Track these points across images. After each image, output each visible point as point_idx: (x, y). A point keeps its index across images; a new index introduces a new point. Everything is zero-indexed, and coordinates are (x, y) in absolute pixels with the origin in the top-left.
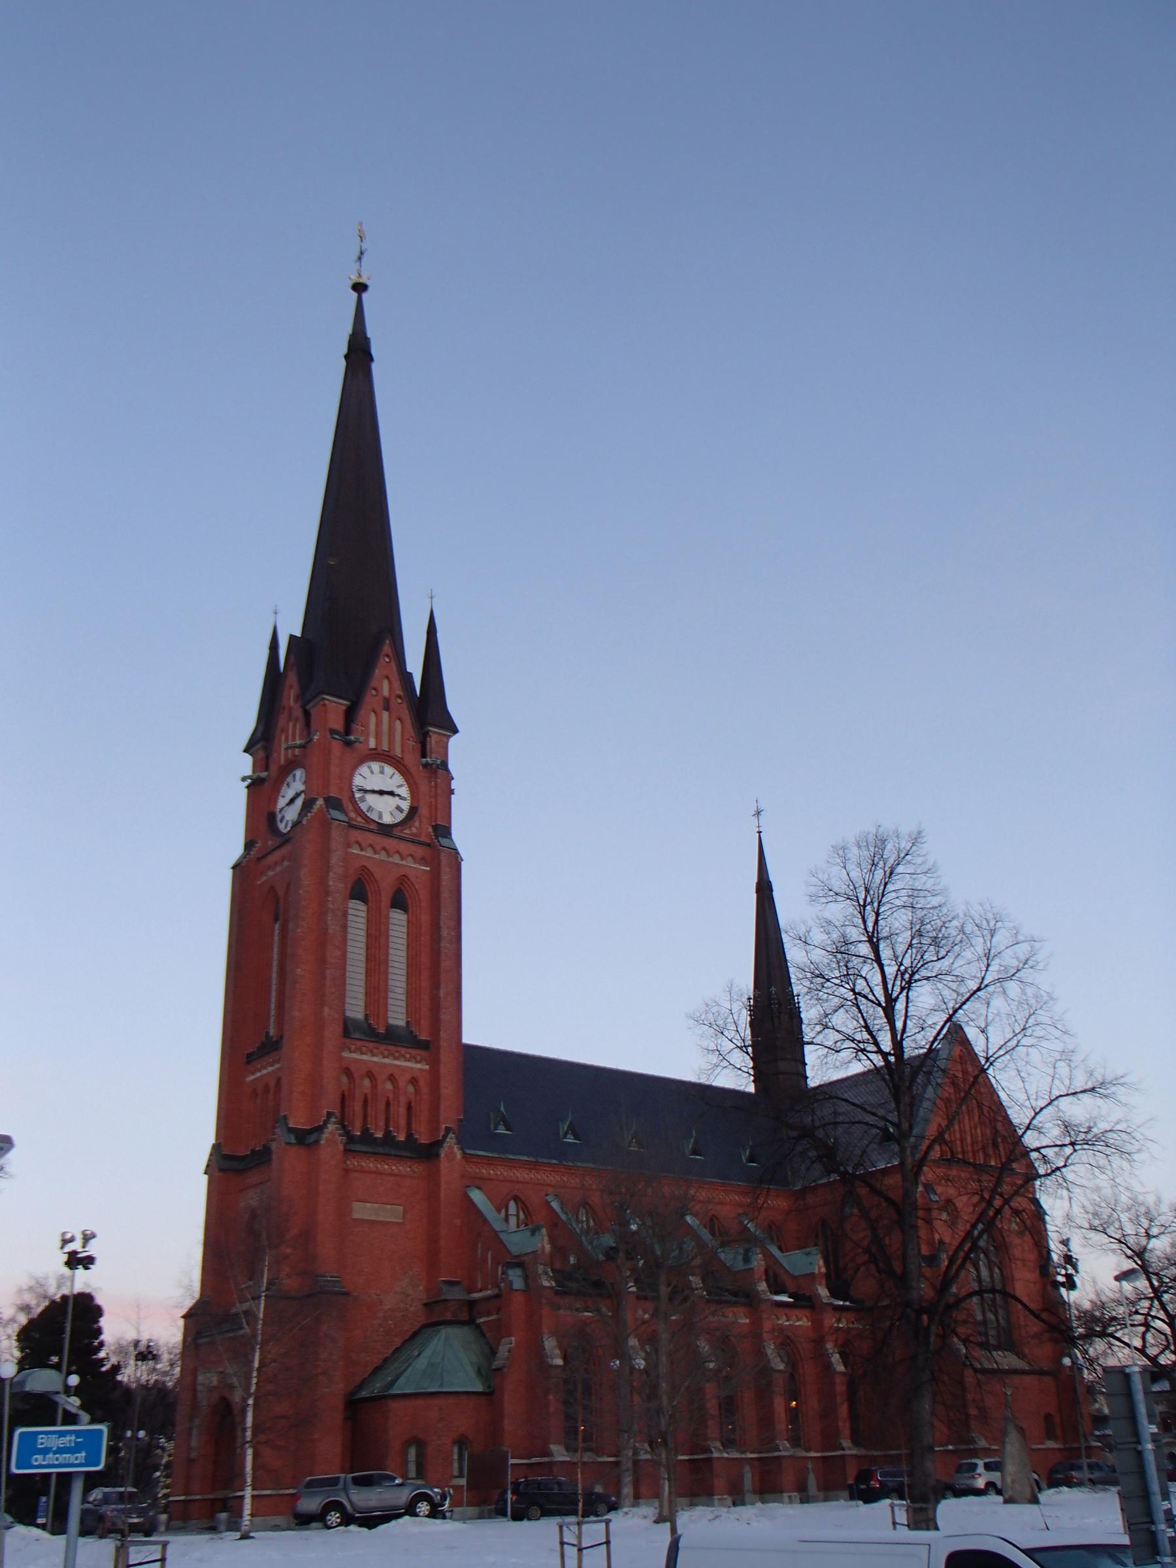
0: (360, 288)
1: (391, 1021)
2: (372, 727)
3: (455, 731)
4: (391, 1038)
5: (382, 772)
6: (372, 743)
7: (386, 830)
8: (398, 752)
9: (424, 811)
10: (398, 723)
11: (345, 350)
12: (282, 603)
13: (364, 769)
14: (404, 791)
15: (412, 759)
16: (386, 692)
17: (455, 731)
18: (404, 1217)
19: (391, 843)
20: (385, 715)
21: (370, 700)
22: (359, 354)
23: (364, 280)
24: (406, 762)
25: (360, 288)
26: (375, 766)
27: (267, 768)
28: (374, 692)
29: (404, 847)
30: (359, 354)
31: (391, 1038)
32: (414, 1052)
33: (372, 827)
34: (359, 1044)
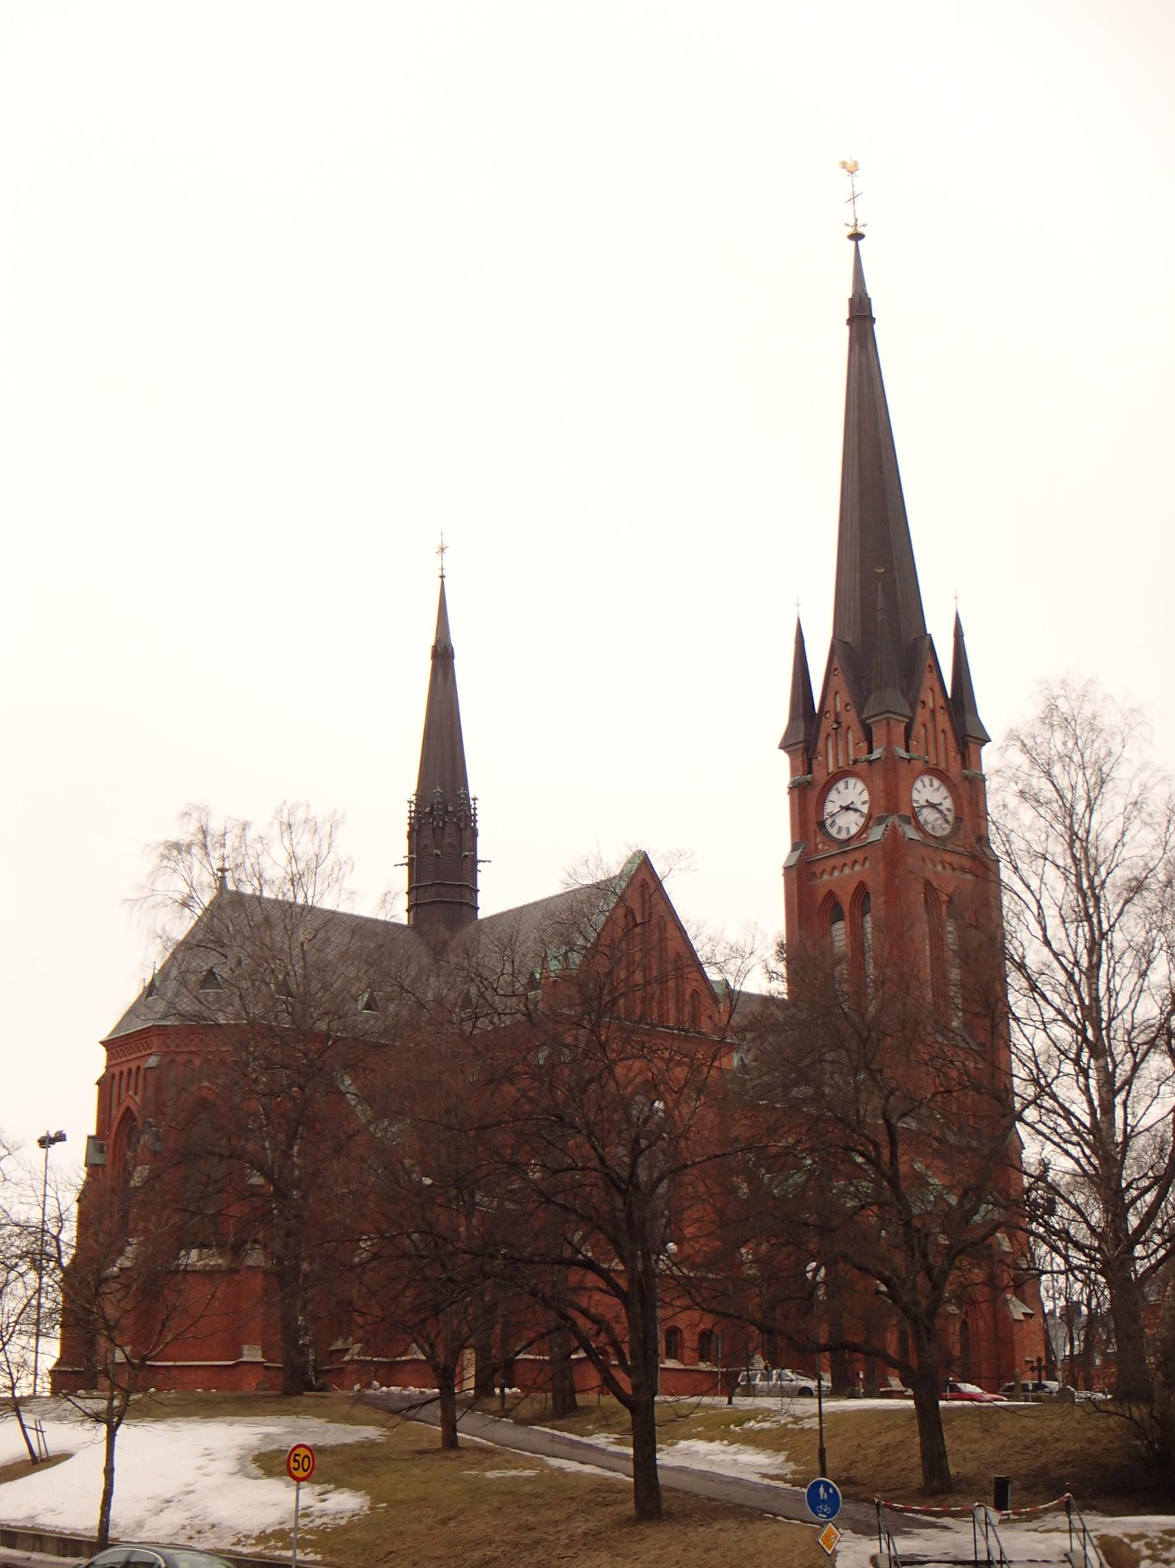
0: (856, 237)
3: (987, 740)
5: (931, 785)
8: (942, 766)
10: (941, 736)
11: (847, 316)
12: (805, 595)
14: (948, 804)
15: (955, 771)
16: (931, 706)
17: (987, 740)
21: (922, 715)
22: (861, 316)
23: (861, 230)
24: (951, 775)
25: (856, 237)
26: (926, 779)
27: (810, 772)
30: (861, 316)
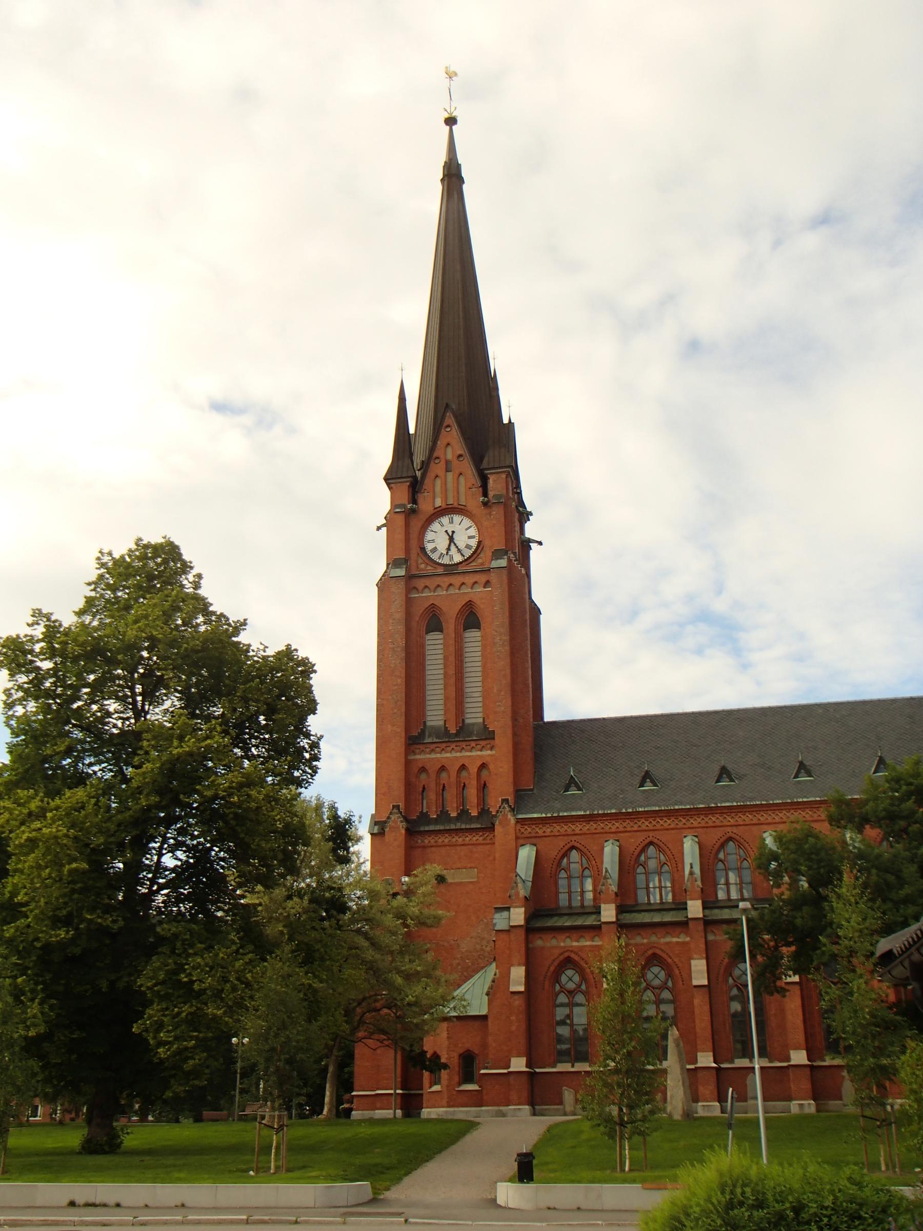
0: (451, 121)
1: (467, 721)
2: (438, 488)
4: (461, 733)
6: (438, 502)
7: (451, 570)
9: (487, 543)
13: (435, 526)
18: (478, 877)
19: (457, 580)
20: (450, 475)
22: (452, 177)
24: (469, 508)
25: (451, 121)
28: (437, 461)
29: (469, 579)
30: (452, 177)
31: (461, 733)
32: (483, 743)
33: (440, 570)
34: (433, 746)
